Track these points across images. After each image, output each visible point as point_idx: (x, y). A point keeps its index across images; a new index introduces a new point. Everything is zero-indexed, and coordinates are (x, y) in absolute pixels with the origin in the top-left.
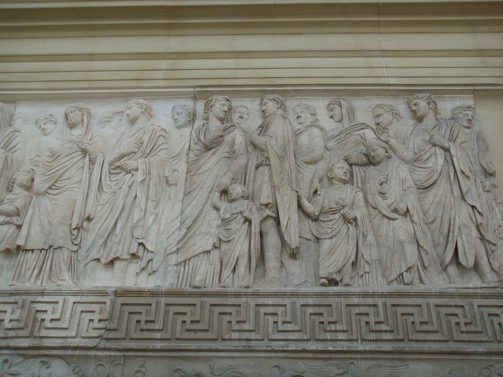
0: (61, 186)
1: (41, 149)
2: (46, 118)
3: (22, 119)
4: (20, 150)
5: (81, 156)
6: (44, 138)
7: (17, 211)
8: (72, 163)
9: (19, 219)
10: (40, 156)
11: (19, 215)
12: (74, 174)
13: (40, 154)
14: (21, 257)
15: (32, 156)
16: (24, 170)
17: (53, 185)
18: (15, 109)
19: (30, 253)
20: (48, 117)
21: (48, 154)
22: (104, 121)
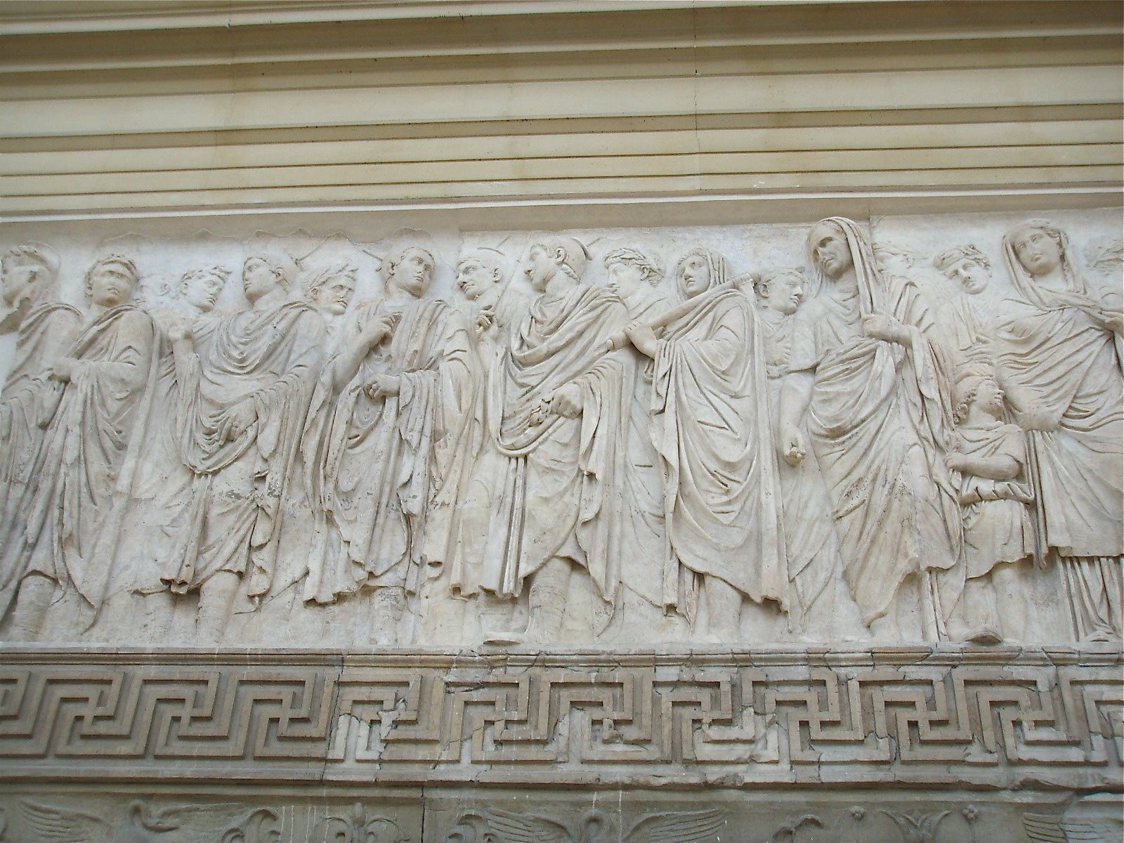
0: (1092, 411)
1: (981, 325)
2: (967, 254)
3: (901, 257)
4: (934, 326)
5: (1103, 341)
6: (971, 298)
7: (1017, 467)
8: (1090, 355)
9: (1025, 486)
10: (985, 342)
11: (1020, 476)
12: (1108, 380)
13: (982, 337)
14: (1067, 577)
15: (966, 343)
16: (983, 373)
17: (1070, 407)
18: (871, 233)
19: (1085, 565)
20: (970, 253)
21: (1007, 336)
22: (1109, 260)
